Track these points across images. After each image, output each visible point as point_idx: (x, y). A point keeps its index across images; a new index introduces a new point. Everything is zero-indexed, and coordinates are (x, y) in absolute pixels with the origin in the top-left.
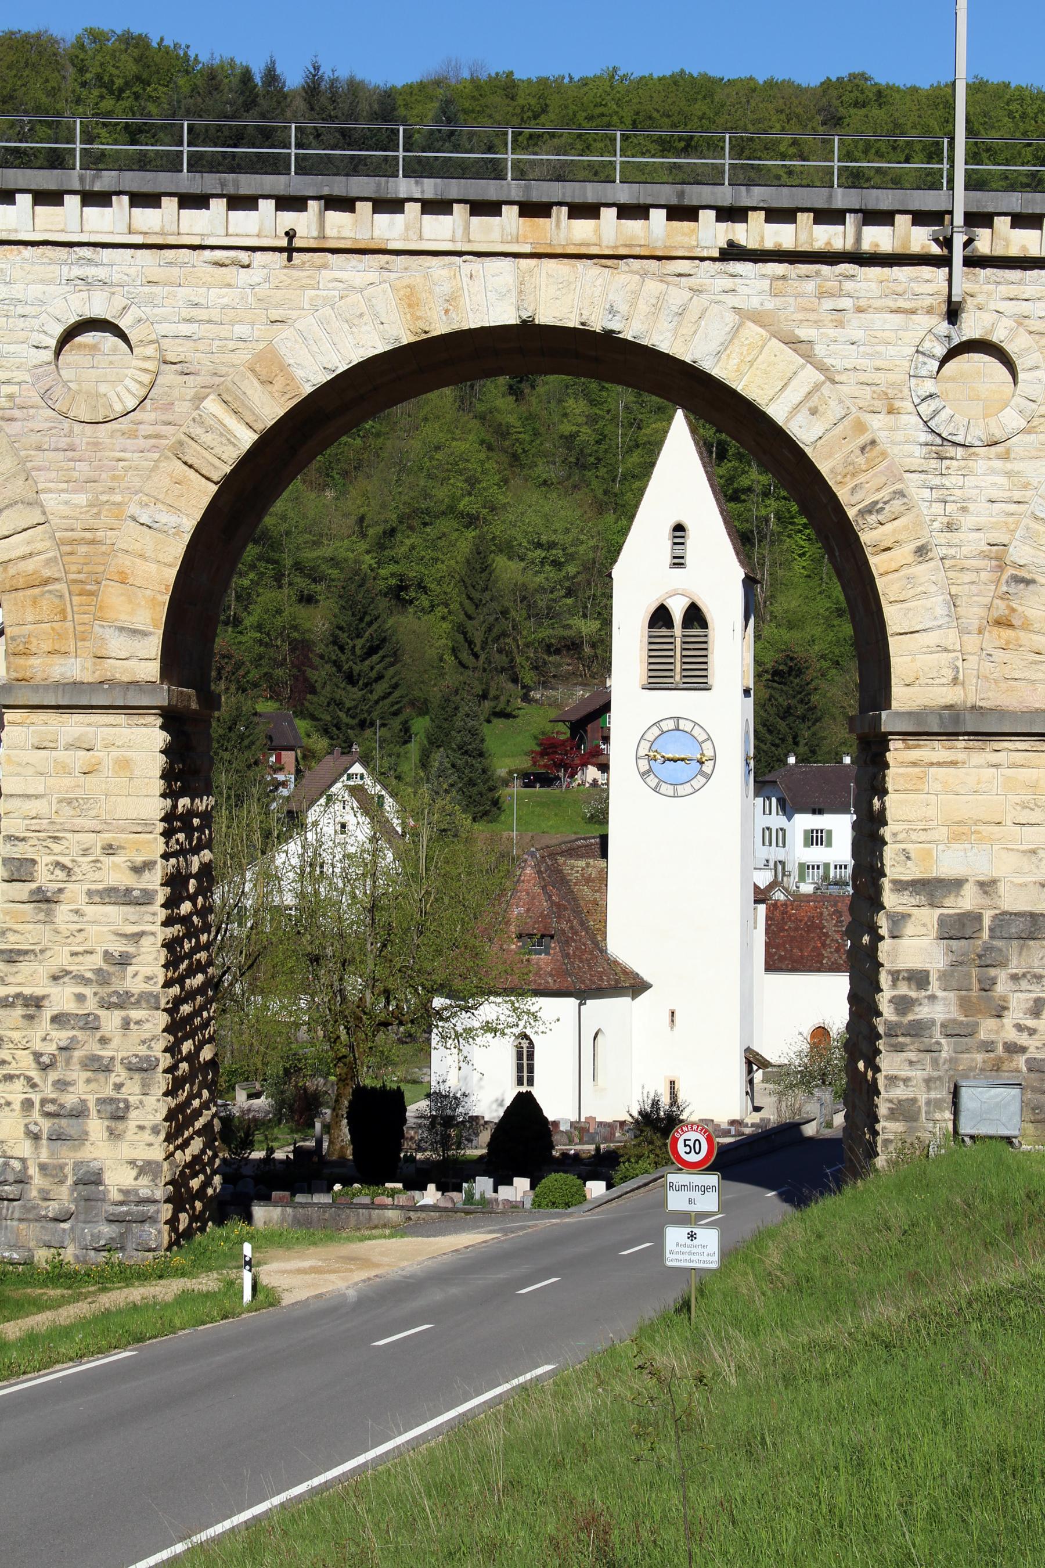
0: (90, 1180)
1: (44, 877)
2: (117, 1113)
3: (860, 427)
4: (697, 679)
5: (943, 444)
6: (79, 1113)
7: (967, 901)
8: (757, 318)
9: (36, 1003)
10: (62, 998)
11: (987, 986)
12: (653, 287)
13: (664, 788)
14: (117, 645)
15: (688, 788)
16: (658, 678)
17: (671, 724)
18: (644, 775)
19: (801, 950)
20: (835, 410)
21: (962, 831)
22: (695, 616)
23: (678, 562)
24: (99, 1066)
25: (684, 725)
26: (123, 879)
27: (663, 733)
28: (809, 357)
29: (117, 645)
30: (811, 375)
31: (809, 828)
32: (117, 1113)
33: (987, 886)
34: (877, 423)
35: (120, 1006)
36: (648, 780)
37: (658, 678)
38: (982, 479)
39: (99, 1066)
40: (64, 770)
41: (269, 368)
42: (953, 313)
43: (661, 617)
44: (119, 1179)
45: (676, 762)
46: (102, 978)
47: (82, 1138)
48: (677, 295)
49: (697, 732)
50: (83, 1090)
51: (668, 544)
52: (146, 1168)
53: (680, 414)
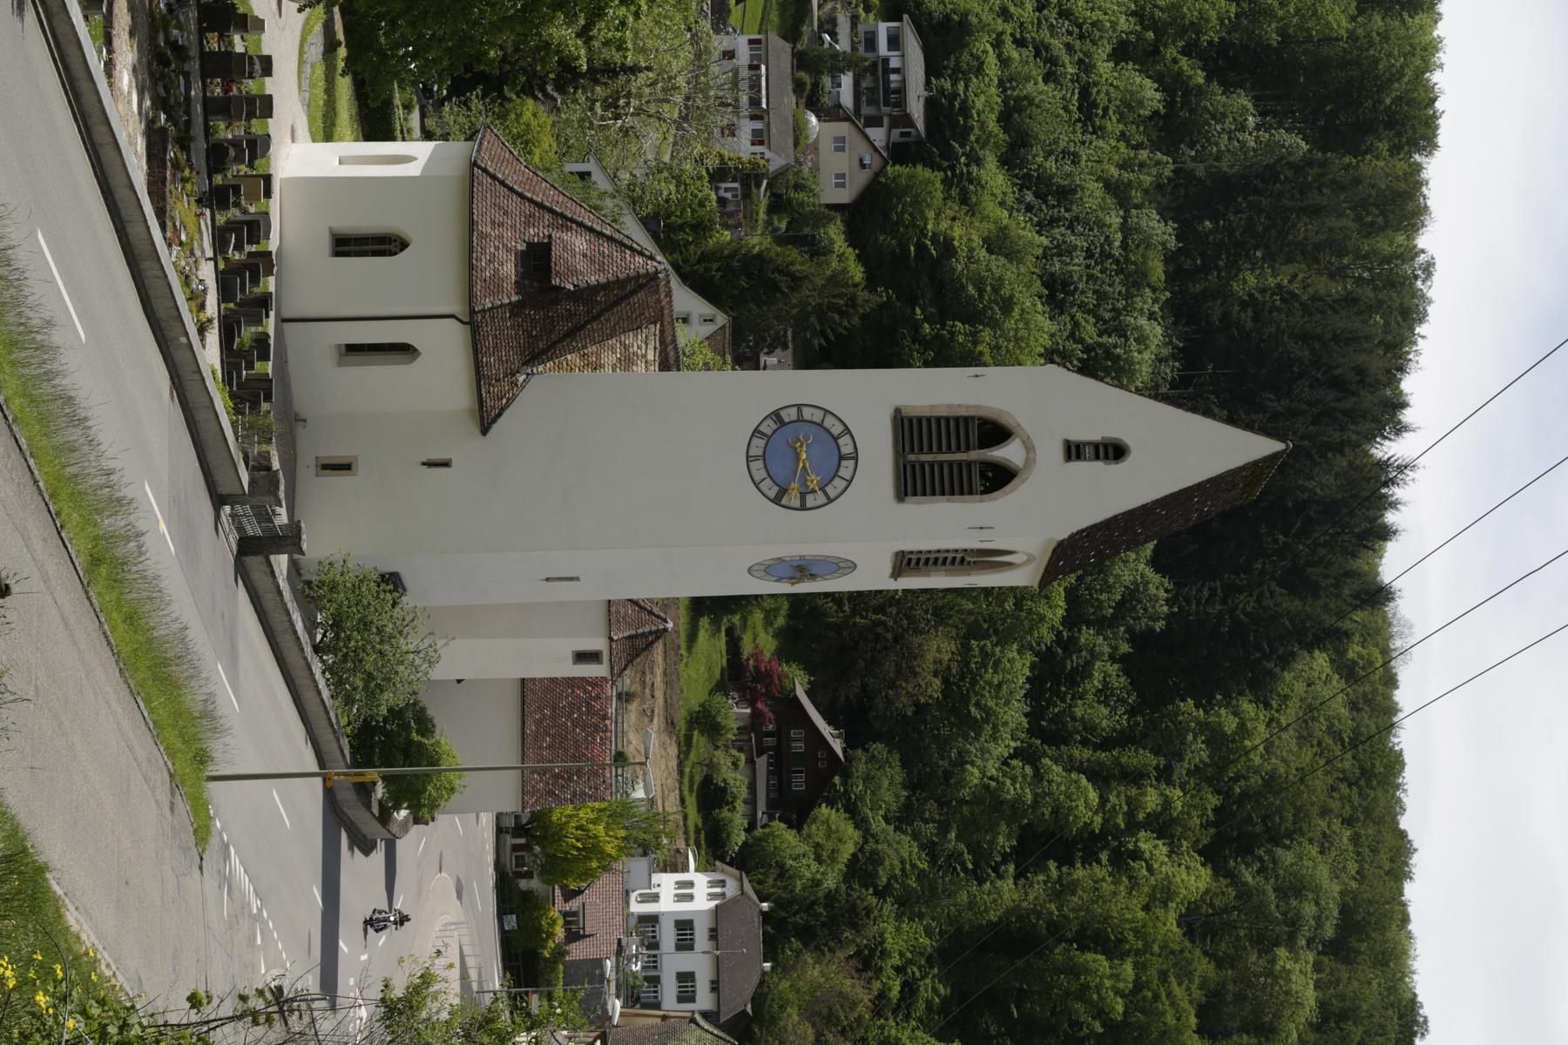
4: (914, 481)
13: (759, 443)
15: (760, 474)
16: (912, 432)
17: (847, 449)
18: (776, 415)
22: (999, 478)
23: (1074, 451)
25: (846, 469)
27: (836, 439)
31: (696, 924)
36: (769, 421)
37: (912, 432)
43: (995, 432)
45: (794, 462)
49: (839, 484)
51: (1095, 436)
53: (1278, 446)
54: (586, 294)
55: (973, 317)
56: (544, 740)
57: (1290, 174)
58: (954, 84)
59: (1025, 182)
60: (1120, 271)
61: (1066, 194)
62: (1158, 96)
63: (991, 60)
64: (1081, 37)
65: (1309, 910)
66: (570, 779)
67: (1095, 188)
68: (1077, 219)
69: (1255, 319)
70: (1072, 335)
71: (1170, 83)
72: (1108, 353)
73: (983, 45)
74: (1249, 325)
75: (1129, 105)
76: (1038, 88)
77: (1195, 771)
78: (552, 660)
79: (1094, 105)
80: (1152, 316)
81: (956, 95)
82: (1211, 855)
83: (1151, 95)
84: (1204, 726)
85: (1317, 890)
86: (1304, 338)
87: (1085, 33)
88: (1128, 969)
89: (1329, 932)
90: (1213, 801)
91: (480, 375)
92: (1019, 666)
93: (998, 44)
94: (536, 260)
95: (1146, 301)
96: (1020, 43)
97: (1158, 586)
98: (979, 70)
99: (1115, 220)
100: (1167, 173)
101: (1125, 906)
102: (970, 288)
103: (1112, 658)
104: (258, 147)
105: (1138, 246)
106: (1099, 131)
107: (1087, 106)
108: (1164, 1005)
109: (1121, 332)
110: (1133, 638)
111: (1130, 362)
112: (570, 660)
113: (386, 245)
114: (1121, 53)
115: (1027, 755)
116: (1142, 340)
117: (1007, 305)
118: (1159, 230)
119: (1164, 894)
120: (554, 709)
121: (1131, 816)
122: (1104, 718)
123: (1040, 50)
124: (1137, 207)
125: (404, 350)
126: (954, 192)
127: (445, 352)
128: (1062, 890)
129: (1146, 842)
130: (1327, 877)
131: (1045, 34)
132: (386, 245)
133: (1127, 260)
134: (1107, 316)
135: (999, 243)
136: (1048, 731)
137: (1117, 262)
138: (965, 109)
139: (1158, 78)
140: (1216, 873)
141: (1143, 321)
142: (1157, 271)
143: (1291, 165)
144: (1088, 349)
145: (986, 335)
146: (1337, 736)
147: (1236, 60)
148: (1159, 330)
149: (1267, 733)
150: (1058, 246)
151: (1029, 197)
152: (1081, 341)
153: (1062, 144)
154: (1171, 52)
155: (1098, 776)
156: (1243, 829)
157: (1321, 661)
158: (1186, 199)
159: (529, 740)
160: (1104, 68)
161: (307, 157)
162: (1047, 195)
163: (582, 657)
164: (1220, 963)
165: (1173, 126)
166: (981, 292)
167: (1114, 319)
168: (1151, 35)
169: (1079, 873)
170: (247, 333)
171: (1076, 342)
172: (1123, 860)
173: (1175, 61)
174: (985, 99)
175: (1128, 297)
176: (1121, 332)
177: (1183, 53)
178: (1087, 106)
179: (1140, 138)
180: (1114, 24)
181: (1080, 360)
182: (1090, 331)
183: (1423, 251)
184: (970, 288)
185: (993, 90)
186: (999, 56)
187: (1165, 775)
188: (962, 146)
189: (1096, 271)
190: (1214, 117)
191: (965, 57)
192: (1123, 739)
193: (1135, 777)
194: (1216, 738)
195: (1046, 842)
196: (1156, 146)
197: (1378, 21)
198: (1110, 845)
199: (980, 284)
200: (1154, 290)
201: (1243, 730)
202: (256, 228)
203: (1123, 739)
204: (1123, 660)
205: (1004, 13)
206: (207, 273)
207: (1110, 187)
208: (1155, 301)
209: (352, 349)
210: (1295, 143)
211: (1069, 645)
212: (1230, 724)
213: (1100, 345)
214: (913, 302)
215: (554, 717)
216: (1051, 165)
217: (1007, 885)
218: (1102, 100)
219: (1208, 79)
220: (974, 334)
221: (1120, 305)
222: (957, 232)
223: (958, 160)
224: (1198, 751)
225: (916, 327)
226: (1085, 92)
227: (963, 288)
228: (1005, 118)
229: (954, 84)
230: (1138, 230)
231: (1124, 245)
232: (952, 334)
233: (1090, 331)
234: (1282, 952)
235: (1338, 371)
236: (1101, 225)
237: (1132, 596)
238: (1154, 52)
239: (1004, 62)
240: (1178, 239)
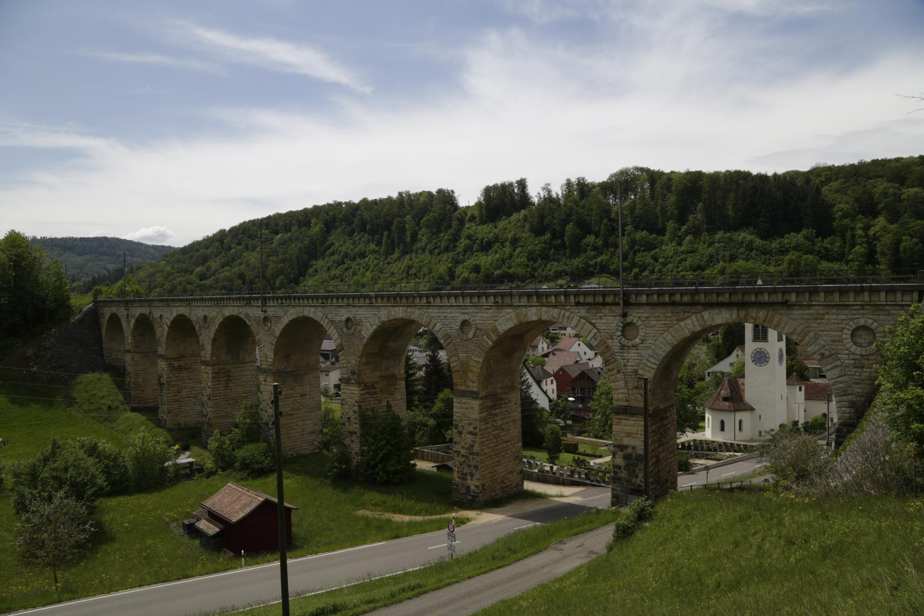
0: (468, 488)
1: (461, 429)
2: (472, 476)
3: (605, 342)
4: (765, 338)
5: (623, 347)
6: (466, 474)
7: (629, 451)
8: (584, 318)
9: (459, 452)
10: (463, 452)
11: (634, 471)
12: (563, 312)
14: (471, 384)
16: (756, 338)
20: (599, 339)
21: (629, 435)
24: (469, 466)
26: (472, 429)
28: (595, 327)
29: (471, 384)
30: (595, 330)
32: (472, 476)
33: (634, 448)
34: (609, 341)
35: (472, 454)
37: (756, 338)
38: (632, 355)
39: (469, 466)
40: (462, 408)
41: (495, 330)
42: (625, 315)
44: (473, 488)
46: (469, 449)
47: (466, 479)
48: (567, 314)
50: (466, 470)
52: (477, 487)
54: (731, 392)
61: (711, 256)
65: (891, 190)
67: (710, 249)
71: (687, 233)
75: (691, 242)
76: (688, 263)
77: (852, 221)
78: (800, 395)
82: (875, 215)
83: (689, 237)
84: (840, 220)
85: (885, 189)
87: (676, 253)
88: (905, 238)
89: (897, 185)
90: (860, 216)
91: (745, 410)
92: (824, 265)
94: (725, 399)
96: (678, 267)
97: (804, 232)
99: (717, 245)
101: (887, 239)
103: (823, 242)
104: (707, 442)
107: (691, 252)
108: (915, 229)
109: (742, 243)
110: (817, 237)
113: (722, 423)
114: (680, 244)
115: (847, 263)
116: (744, 238)
117: (736, 271)
118: (719, 235)
119: (884, 229)
121: (863, 237)
122: (837, 244)
123: (680, 262)
125: (740, 421)
127: (740, 416)
128: (883, 254)
129: (871, 232)
130: (881, 186)
132: (722, 423)
135: (722, 272)
136: (841, 257)
139: (686, 236)
140: (880, 214)
142: (728, 235)
146: (845, 183)
147: (682, 220)
149: (842, 204)
154: (680, 234)
155: (853, 246)
156: (869, 209)
157: (824, 190)
158: (712, 231)
160: (683, 248)
161: (708, 433)
162: (712, 260)
163: (800, 390)
164: (906, 212)
165: (696, 232)
169: (878, 249)
170: (736, 448)
172: (876, 238)
176: (742, 243)
178: (691, 252)
182: (742, 250)
187: (853, 229)
192: (843, 238)
193: (853, 236)
194: (844, 216)
195: (870, 258)
196: (700, 236)
197: (673, 188)
198: (871, 243)
201: (842, 210)
202: (720, 445)
203: (843, 238)
204: (823, 239)
205: (672, 271)
206: (727, 454)
207: (709, 246)
209: (740, 429)
210: (700, 205)
211: (819, 252)
212: (840, 213)
217: (881, 267)
224: (846, 221)
228: (695, 270)
233: (742, 250)
234: (903, 197)
237: (806, 238)
238: (680, 237)
239: (682, 271)
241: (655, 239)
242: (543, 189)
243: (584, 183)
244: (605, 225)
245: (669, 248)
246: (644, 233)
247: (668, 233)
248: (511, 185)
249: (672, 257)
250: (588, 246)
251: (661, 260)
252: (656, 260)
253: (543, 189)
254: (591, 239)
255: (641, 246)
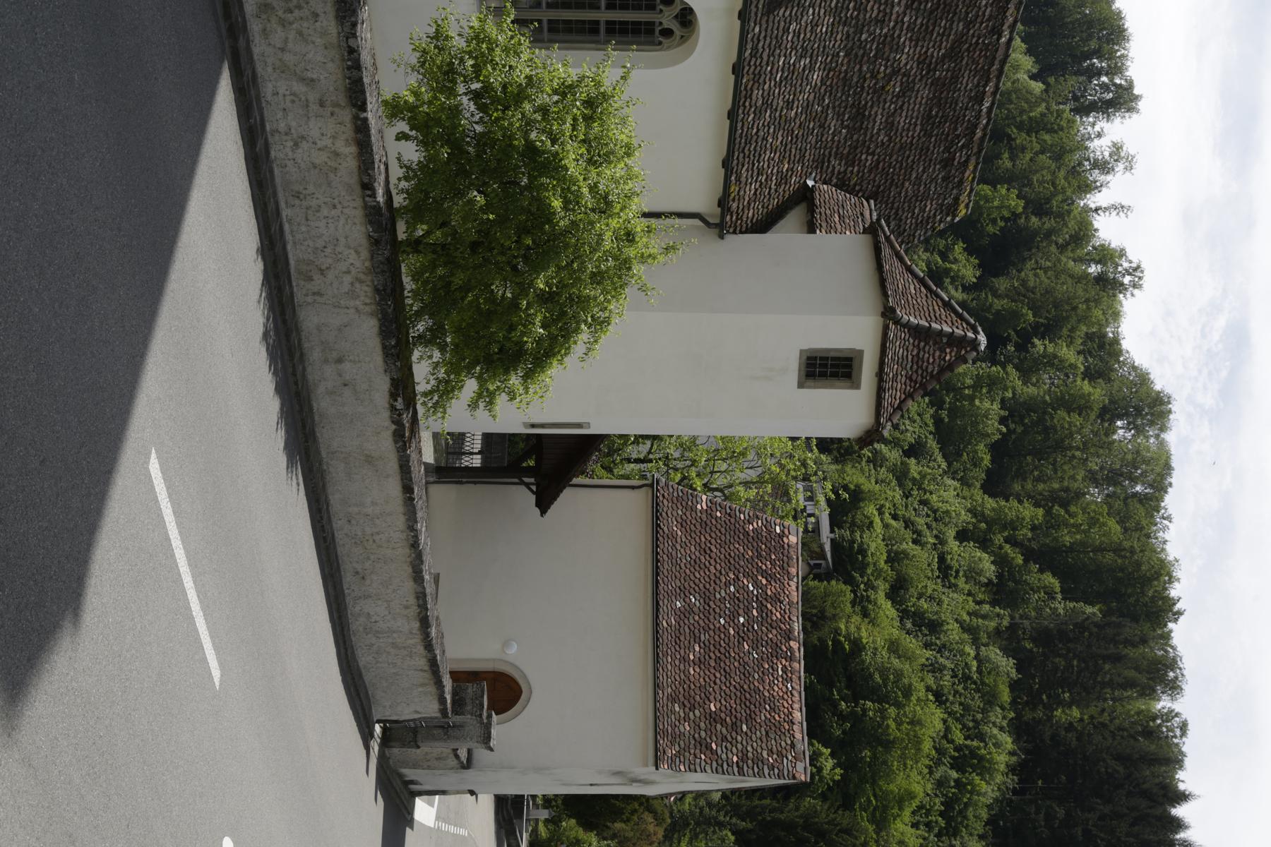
19: (700, 662)
55: (881, 697)
56: (690, 648)
57: (1095, 630)
58: (852, 532)
59: (904, 614)
60: (977, 690)
61: (935, 627)
62: (993, 568)
63: (877, 520)
64: (936, 520)
66: (735, 727)
68: (944, 646)
69: (1078, 739)
70: (945, 737)
72: (973, 753)
73: (871, 510)
74: (1074, 743)
75: (972, 574)
76: (908, 546)
79: (949, 567)
80: (1001, 729)
81: (853, 542)
83: (988, 568)
86: (1119, 758)
87: (938, 516)
93: (880, 511)
95: (996, 715)
96: (895, 517)
98: (871, 525)
100: (1005, 623)
102: (877, 676)
105: (989, 673)
106: (953, 587)
111: (990, 761)
112: (793, 375)
114: (962, 536)
116: (997, 745)
117: (908, 692)
120: (706, 598)
123: (908, 524)
124: (986, 645)
126: (858, 609)
131: (911, 514)
133: (983, 683)
134: (971, 724)
135: (894, 647)
137: (975, 683)
138: (863, 551)
141: (995, 731)
142: (1006, 696)
143: (1096, 625)
144: (957, 749)
145: (892, 711)
148: (1009, 740)
150: (931, 665)
151: (909, 625)
152: (952, 742)
153: (930, 591)
159: (665, 638)
160: (953, 545)
165: (1004, 591)
166: (885, 680)
167: (975, 728)
168: (983, 525)
171: (948, 742)
173: (1001, 547)
174: (875, 545)
175: (984, 711)
176: (981, 737)
177: (1007, 540)
178: (944, 570)
179: (980, 596)
180: (958, 515)
181: (952, 757)
183: (1177, 715)
184: (877, 676)
185: (879, 541)
186: (882, 520)
188: (862, 576)
189: (960, 688)
190: (1032, 589)
191: (859, 516)
196: (993, 603)
199: (884, 671)
200: (1003, 708)
207: (965, 628)
208: (1004, 718)
213: (966, 746)
214: (831, 685)
215: (707, 613)
216: (924, 604)
218: (955, 564)
219: (1026, 561)
220: (882, 711)
221: (979, 716)
222: (864, 634)
223: (858, 586)
225: (835, 705)
226: (942, 559)
227: (871, 676)
229: (852, 532)
230: (989, 660)
231: (979, 671)
232: (864, 711)
235: (1145, 786)
236: (962, 653)
239: (886, 526)
240: (1018, 671)
241: (976, 463)
242: (1117, 148)
243: (1121, 287)
244: (1016, 315)
245: (952, 498)
246: (993, 427)
247: (990, 503)
248: (1116, 68)
249: (924, 503)
250: (944, 256)
251: (914, 467)
252: (915, 451)
253: (1117, 148)
254: (968, 270)
255: (953, 412)
